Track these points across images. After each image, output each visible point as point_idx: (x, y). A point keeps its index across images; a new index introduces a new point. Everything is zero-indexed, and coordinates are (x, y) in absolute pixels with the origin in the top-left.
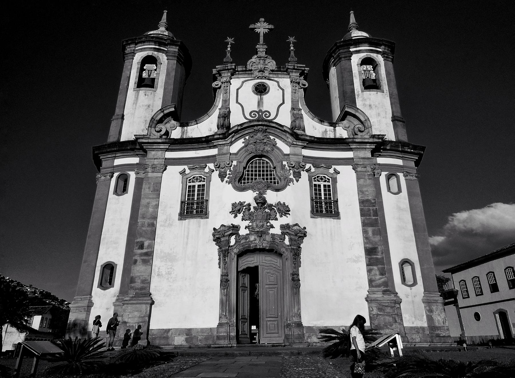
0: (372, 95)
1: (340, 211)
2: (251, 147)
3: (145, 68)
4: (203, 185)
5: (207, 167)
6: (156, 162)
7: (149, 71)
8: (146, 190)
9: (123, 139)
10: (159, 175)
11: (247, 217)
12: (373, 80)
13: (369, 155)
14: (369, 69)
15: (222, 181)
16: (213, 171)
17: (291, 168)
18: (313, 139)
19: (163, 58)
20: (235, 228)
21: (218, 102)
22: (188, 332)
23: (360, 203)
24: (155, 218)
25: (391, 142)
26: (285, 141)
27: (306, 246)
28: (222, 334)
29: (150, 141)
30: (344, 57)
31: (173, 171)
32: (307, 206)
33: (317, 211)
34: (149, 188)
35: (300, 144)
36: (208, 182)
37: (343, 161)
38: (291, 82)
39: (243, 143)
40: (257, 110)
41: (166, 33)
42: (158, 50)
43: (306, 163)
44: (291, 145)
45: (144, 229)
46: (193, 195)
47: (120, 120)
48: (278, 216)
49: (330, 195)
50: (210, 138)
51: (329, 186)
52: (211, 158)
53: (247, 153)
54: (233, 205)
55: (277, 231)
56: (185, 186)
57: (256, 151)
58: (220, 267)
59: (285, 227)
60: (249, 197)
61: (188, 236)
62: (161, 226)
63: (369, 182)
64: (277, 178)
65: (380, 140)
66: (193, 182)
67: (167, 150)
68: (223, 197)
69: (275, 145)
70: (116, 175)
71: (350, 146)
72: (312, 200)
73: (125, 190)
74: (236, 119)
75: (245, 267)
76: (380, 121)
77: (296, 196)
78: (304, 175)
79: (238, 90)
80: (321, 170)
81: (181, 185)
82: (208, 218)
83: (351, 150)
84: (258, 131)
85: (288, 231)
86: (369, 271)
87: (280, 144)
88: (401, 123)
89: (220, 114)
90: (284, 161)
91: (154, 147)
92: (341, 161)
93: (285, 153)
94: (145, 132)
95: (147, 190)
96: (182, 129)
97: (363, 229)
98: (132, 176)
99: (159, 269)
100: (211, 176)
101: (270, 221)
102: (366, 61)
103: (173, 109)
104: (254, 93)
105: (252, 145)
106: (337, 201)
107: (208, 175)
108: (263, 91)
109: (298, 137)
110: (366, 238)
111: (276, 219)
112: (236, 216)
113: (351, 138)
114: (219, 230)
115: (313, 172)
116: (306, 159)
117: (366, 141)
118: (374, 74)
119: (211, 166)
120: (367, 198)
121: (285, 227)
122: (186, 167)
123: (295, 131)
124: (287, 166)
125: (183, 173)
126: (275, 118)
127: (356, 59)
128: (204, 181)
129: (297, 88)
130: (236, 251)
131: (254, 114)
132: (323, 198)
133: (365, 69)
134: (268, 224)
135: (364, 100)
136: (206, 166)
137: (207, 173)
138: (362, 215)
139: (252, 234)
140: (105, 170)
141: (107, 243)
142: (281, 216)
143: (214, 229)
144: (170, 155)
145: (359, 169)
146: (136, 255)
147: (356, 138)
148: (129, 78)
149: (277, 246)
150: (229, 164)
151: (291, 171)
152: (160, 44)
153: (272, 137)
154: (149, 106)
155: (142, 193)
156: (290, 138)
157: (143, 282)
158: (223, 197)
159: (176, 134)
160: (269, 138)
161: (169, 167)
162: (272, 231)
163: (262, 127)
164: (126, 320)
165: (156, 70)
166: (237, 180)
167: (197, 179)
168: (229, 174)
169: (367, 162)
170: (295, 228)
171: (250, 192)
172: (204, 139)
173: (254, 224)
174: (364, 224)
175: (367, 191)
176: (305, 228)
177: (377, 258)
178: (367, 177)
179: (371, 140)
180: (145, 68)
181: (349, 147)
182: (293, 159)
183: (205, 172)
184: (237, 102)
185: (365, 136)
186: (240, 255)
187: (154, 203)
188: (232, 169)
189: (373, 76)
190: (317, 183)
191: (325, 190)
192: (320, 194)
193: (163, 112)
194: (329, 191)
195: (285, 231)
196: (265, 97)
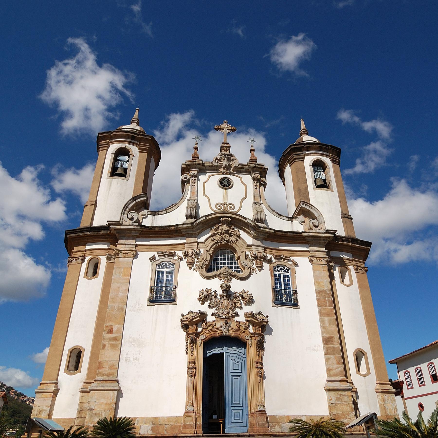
0: (323, 192)
2: (217, 238)
4: (172, 272)
6: (127, 248)
8: (116, 275)
9: (95, 224)
11: (214, 304)
15: (190, 268)
16: (181, 259)
18: (273, 231)
20: (203, 315)
22: (154, 421)
23: (316, 293)
25: (341, 237)
26: (247, 232)
28: (189, 423)
29: (122, 227)
30: (298, 159)
31: (144, 257)
33: (277, 300)
36: (177, 269)
41: (138, 128)
42: (132, 143)
43: (267, 253)
45: (113, 313)
46: (162, 282)
47: (94, 206)
49: (289, 284)
50: (179, 226)
53: (213, 243)
55: (241, 318)
58: (187, 354)
60: (215, 285)
62: (130, 311)
64: (241, 267)
65: (333, 235)
66: (162, 268)
68: (191, 285)
69: (239, 237)
70: (87, 258)
71: (306, 240)
73: (95, 273)
75: (211, 354)
77: (258, 285)
81: (151, 271)
85: (251, 319)
86: (327, 360)
89: (188, 205)
92: (299, 253)
93: (248, 243)
94: (119, 221)
97: (320, 319)
98: (103, 260)
99: (127, 354)
103: (145, 198)
104: (220, 187)
105: (217, 235)
106: (296, 293)
108: (227, 185)
110: (323, 327)
111: (241, 308)
112: (203, 303)
113: (306, 232)
114: (187, 316)
118: (324, 175)
124: (250, 256)
125: (152, 259)
126: (239, 210)
129: (258, 184)
130: (202, 337)
132: (283, 288)
137: (176, 260)
138: (319, 305)
143: (183, 315)
145: (315, 261)
146: (104, 339)
150: (196, 253)
151: (254, 262)
155: (113, 278)
157: (111, 367)
163: (227, 218)
164: (93, 407)
165: (128, 161)
166: (204, 267)
167: (166, 265)
168: (197, 262)
170: (259, 317)
171: (216, 279)
172: (173, 228)
173: (221, 312)
174: (321, 314)
175: (323, 282)
178: (322, 269)
179: (324, 235)
182: (256, 251)
185: (319, 232)
187: (125, 287)
189: (323, 178)
190: (277, 273)
191: (284, 280)
192: (280, 284)
194: (288, 281)
195: (249, 319)
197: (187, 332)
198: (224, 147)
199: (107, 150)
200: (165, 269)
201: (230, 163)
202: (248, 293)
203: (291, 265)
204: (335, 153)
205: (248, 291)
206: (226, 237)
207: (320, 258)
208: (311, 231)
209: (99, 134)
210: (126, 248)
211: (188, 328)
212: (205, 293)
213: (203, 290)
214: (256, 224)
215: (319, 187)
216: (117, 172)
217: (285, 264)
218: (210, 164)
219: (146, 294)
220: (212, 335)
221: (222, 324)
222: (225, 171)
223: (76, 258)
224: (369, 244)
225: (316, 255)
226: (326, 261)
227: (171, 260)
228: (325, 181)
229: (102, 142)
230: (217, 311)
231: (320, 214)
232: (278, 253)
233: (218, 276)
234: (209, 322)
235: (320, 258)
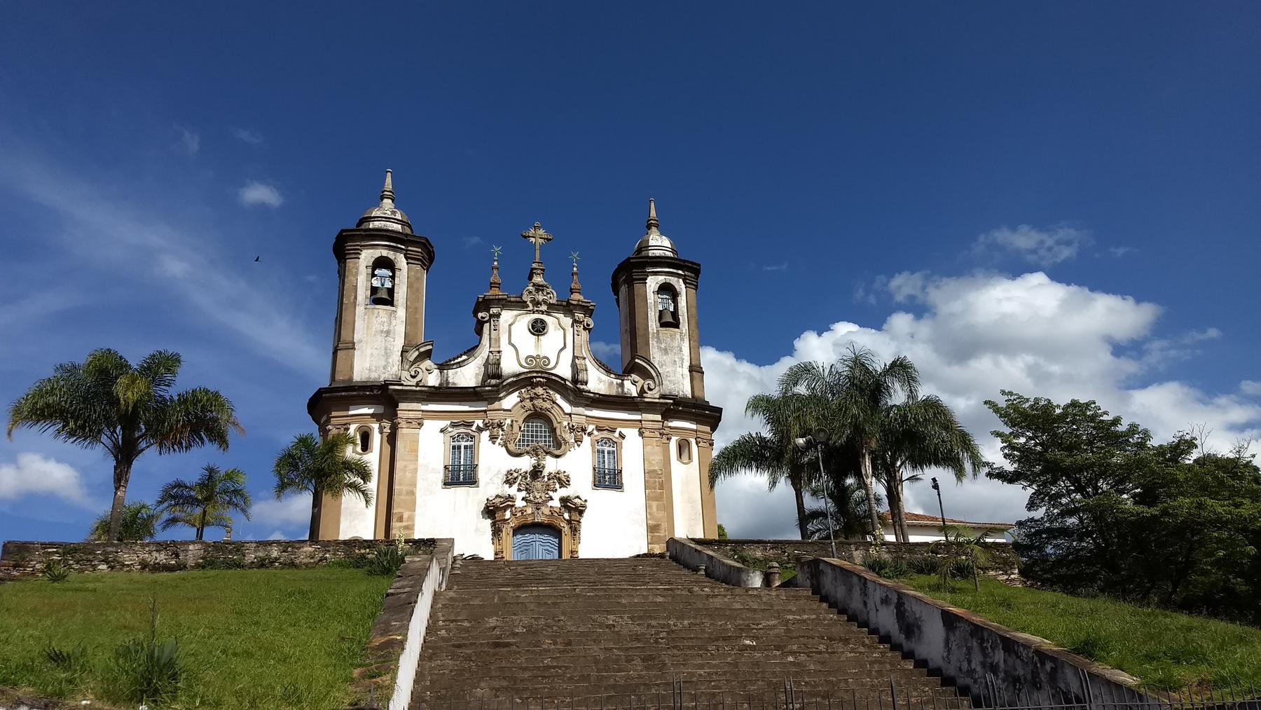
4: (471, 447)
6: (411, 415)
13: (659, 417)
16: (480, 430)
19: (401, 261)
24: (415, 485)
27: (586, 522)
32: (589, 477)
38: (575, 321)
44: (572, 403)
48: (557, 486)
54: (509, 473)
55: (556, 503)
59: (565, 501)
60: (526, 463)
63: (658, 449)
74: (510, 366)
76: (675, 372)
78: (586, 439)
102: (665, 289)
121: (565, 501)
127: (653, 283)
135: (659, 341)
141: (351, 514)
145: (647, 433)
148: (356, 288)
154: (388, 333)
158: (494, 461)
159: (433, 380)
161: (426, 422)
170: (577, 501)
171: (527, 458)
174: (648, 498)
184: (510, 343)
186: (518, 530)
204: (692, 271)
206: (538, 402)
207: (652, 430)
209: (342, 231)
215: (664, 325)
216: (379, 295)
219: (440, 476)
224: (719, 410)
228: (675, 314)
232: (602, 424)
233: (528, 453)
235: (652, 430)
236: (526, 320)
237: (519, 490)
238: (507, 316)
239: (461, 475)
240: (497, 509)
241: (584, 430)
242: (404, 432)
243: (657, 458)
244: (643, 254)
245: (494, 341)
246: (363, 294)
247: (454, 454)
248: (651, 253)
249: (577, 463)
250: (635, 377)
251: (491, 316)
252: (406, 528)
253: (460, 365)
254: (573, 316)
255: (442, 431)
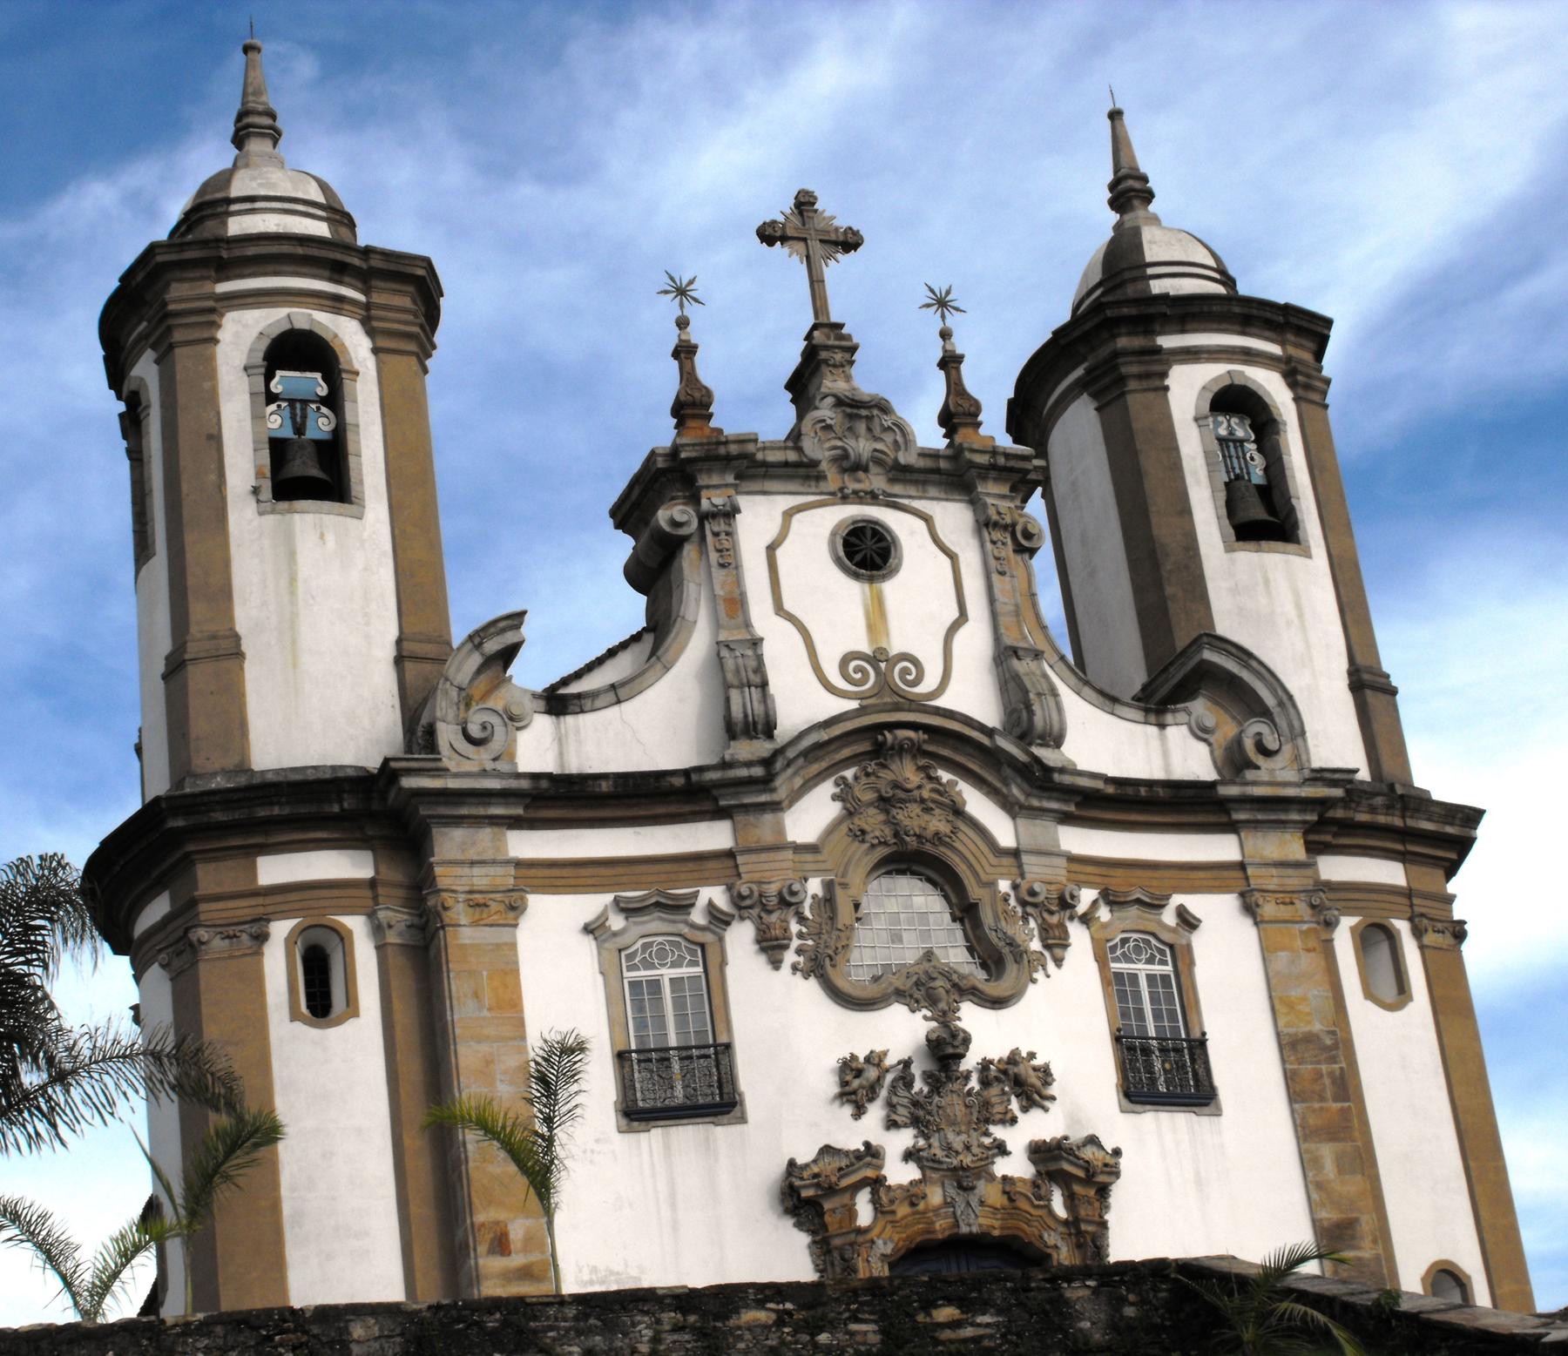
1: (1219, 1078)
3: (276, 386)
5: (702, 901)
6: (481, 878)
7: (292, 402)
10: (501, 935)
11: (902, 1114)
12: (1258, 487)
14: (1240, 433)
15: (776, 964)
16: (719, 920)
17: (1029, 909)
21: (692, 603)
29: (452, 784)
30: (1140, 377)
34: (476, 995)
35: (1054, 805)
37: (1208, 874)
39: (835, 798)
40: (865, 647)
43: (1080, 884)
48: (1014, 1105)
49: (1172, 1015)
51: (1165, 978)
52: (712, 864)
55: (1015, 1165)
56: (615, 984)
57: (896, 835)
60: (899, 1032)
61: (673, 1195)
66: (649, 965)
67: (516, 823)
69: (957, 811)
70: (280, 929)
72: (1117, 1040)
78: (1079, 938)
79: (771, 549)
80: (1134, 911)
81: (600, 979)
82: (743, 1120)
83: (1231, 827)
84: (900, 750)
87: (978, 804)
88: (1388, 697)
90: (1003, 876)
91: (464, 811)
92: (1201, 874)
95: (471, 1004)
96: (558, 727)
100: (721, 940)
101: (992, 1129)
103: (509, 638)
106: (1199, 1046)
107: (708, 938)
109: (1051, 780)
111: (1014, 1121)
112: (859, 1112)
114: (816, 1169)
115: (1105, 926)
116: (1076, 867)
117: (1291, 792)
119: (714, 894)
120: (1304, 1028)
122: (608, 898)
123: (1036, 750)
124: (1012, 902)
127: (1187, 387)
128: (695, 964)
130: (884, 1247)
131: (858, 669)
132: (1152, 1032)
133: (1223, 432)
134: (987, 1141)
136: (695, 895)
138: (1294, 1096)
139: (933, 1183)
140: (220, 905)
142: (1025, 1109)
144: (529, 845)
145: (1269, 909)
147: (1254, 783)
148: (216, 439)
149: (1028, 1223)
151: (1032, 924)
152: (338, 271)
153: (945, 776)
156: (1019, 780)
160: (937, 780)
161: (539, 904)
162: (1002, 1167)
163: (911, 734)
167: (662, 954)
168: (800, 936)
169: (1295, 880)
171: (898, 1011)
172: (679, 782)
174: (1305, 1133)
175: (1304, 999)
176: (1117, 1153)
177: (1359, 1259)
178: (1298, 943)
180: (276, 386)
181: (1224, 819)
183: (693, 926)
188: (807, 913)
191: (1154, 999)
192: (1140, 1013)
193: (478, 646)
195: (1053, 1167)
196: (891, 588)
197: (813, 1232)
198: (827, 348)
199: (215, 341)
200: (663, 971)
201: (879, 446)
202: (1038, 1062)
203: (1173, 930)
205: (1032, 1055)
207: (1286, 897)
208: (1250, 775)
210: (476, 881)
211: (820, 1213)
212: (872, 1073)
213: (853, 1057)
214: (1037, 760)
217: (1152, 927)
218: (792, 456)
220: (919, 1239)
221: (952, 1192)
222: (857, 486)
223: (231, 931)
225: (1272, 884)
226: (1313, 907)
227: (686, 930)
229: (180, 293)
230: (921, 1142)
231: (1285, 698)
232: (1118, 881)
234: (900, 1187)
236: (822, 523)
237: (891, 1124)
238: (757, 517)
239: (683, 1084)
240: (831, 1190)
241: (1066, 904)
242: (465, 935)
243: (1316, 993)
244: (1131, 291)
245: (735, 604)
246: (242, 464)
247: (639, 1007)
248: (1157, 287)
249: (1059, 1020)
250: (1200, 707)
251: (703, 518)
252: (526, 1273)
253: (618, 693)
254: (975, 502)
255: (588, 929)
